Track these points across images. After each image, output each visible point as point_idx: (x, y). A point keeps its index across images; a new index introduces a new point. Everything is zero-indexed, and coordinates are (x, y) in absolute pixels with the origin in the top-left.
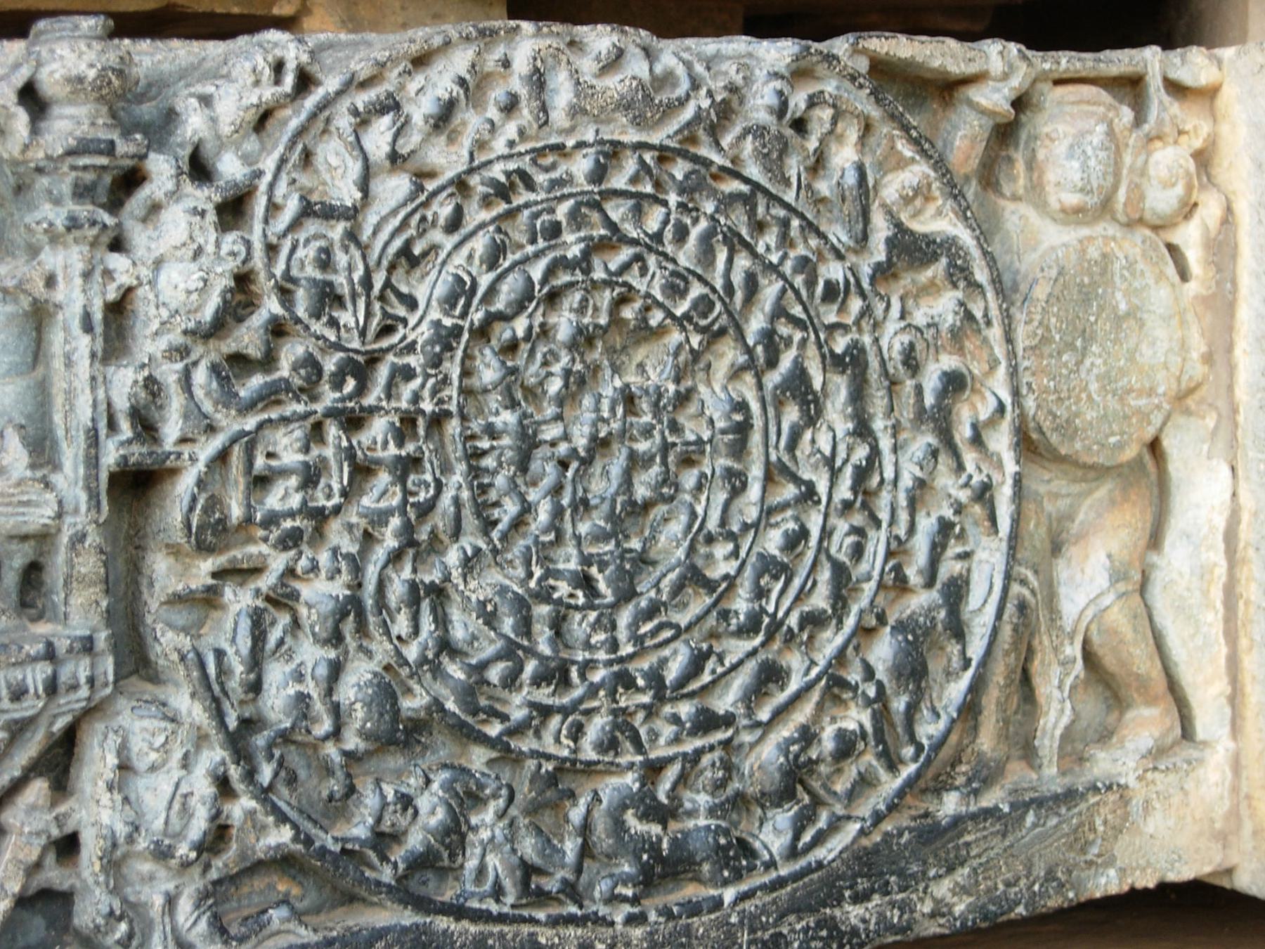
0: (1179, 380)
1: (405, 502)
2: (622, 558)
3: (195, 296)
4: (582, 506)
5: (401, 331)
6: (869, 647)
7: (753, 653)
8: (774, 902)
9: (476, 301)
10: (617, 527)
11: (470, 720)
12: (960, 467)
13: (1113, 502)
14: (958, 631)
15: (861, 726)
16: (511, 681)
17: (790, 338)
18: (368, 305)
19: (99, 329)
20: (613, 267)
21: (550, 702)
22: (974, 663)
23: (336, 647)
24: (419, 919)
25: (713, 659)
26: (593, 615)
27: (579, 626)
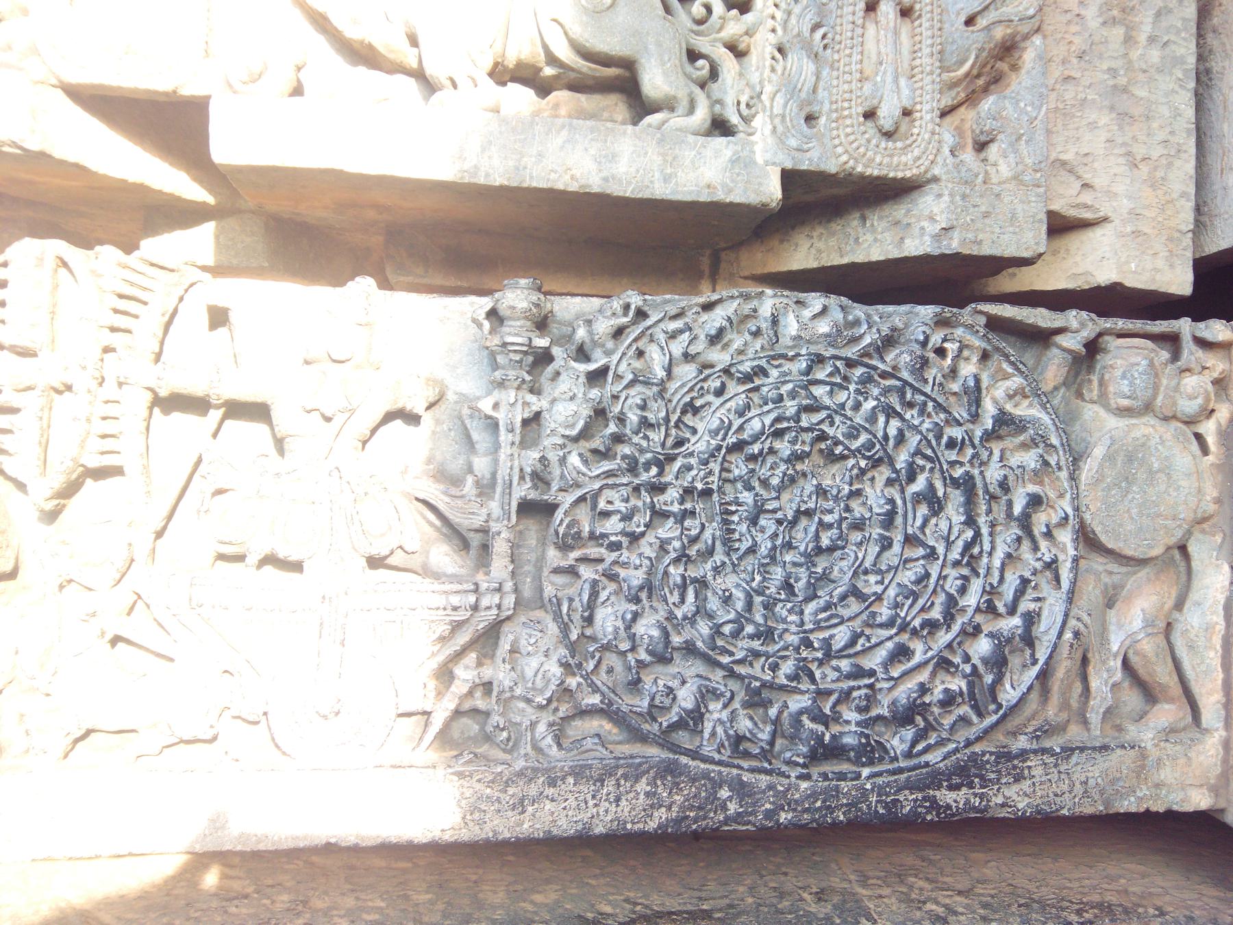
0: (1195, 512)
1: (682, 533)
2: (810, 577)
3: (570, 418)
4: (789, 546)
5: (687, 445)
7: (890, 638)
8: (895, 781)
9: (730, 433)
11: (710, 653)
12: (1036, 548)
13: (1149, 580)
14: (1029, 640)
15: (960, 688)
16: (736, 634)
19: (518, 431)
20: (814, 421)
22: (1041, 662)
23: (636, 604)
24: (671, 756)
26: (789, 605)
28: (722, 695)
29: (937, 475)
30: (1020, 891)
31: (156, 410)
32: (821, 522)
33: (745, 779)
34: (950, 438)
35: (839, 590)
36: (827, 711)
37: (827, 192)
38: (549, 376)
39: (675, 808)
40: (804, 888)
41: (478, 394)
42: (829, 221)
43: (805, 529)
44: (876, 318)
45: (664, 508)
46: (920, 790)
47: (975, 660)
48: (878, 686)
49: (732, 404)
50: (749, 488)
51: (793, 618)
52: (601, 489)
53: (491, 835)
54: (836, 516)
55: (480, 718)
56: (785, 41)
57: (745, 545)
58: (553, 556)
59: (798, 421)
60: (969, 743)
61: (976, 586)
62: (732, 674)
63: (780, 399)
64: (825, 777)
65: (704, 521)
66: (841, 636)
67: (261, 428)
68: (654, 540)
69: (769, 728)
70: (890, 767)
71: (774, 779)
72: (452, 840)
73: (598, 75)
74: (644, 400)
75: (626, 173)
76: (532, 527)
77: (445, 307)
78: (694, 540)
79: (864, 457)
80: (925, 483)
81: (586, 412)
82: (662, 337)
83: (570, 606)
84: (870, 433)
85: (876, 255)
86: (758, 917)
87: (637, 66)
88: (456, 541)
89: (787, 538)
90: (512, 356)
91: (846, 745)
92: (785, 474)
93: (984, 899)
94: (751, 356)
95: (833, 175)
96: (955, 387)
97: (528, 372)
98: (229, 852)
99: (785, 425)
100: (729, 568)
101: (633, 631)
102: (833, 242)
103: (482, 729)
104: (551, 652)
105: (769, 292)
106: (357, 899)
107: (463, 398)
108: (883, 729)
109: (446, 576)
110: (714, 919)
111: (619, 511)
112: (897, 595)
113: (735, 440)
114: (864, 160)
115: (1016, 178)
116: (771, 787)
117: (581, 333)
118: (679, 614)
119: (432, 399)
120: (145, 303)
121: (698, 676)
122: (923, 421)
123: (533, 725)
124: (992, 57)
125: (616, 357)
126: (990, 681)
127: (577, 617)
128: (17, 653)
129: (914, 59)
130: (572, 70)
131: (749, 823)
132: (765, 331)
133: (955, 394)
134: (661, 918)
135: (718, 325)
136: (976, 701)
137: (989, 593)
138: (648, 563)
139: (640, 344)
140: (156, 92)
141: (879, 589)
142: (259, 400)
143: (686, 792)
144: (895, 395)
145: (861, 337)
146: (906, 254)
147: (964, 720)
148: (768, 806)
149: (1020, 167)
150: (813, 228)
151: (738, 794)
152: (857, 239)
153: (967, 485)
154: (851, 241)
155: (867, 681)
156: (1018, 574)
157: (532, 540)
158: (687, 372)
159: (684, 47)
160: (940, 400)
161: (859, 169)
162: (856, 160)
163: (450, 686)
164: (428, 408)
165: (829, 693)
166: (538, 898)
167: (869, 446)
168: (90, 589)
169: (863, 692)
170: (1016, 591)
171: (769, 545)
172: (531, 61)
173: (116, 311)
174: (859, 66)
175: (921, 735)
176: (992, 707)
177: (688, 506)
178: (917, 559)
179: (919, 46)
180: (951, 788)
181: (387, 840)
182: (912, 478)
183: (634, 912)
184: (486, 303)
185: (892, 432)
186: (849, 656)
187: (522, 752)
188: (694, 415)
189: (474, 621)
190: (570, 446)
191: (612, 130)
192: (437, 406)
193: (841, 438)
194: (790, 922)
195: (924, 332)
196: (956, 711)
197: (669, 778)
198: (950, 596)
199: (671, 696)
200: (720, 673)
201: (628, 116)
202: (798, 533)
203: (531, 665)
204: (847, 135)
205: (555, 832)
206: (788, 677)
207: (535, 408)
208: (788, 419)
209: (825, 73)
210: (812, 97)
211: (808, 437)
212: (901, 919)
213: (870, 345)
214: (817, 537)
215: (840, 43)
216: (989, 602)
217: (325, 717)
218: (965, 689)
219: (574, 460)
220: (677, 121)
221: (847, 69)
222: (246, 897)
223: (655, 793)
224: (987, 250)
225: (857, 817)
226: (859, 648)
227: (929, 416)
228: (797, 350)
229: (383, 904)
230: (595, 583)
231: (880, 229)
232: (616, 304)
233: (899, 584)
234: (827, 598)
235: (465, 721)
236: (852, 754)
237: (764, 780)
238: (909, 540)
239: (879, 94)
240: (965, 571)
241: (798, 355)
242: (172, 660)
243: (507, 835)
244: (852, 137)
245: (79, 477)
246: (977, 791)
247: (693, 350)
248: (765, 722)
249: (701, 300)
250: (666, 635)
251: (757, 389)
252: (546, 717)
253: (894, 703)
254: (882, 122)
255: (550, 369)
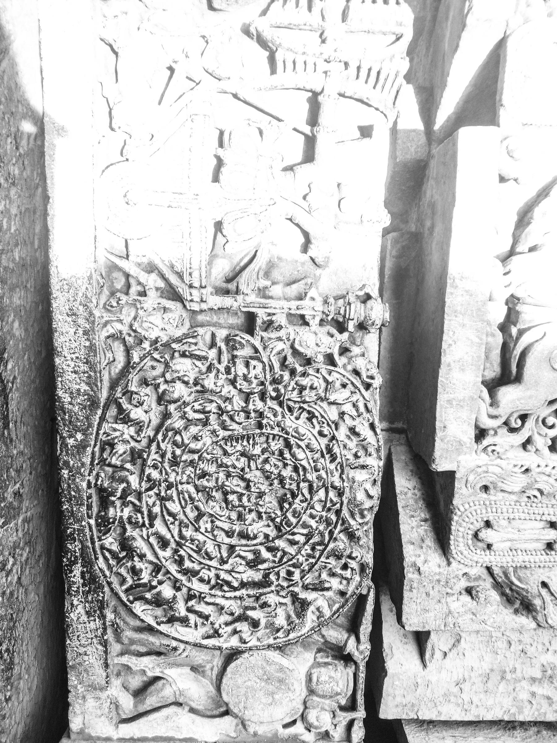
1: (236, 411)
2: (210, 488)
4: (228, 475)
6: (170, 583)
9: (296, 440)
10: (221, 488)
11: (164, 428)
12: (227, 624)
14: (171, 620)
16: (175, 443)
17: (276, 557)
18: (298, 402)
19: (299, 312)
21: (167, 458)
22: (158, 627)
24: (102, 404)
25: (173, 520)
26: (192, 476)
27: (189, 470)
28: (139, 435)
29: (271, 565)
30: (20, 615)
31: (310, 94)
32: (242, 495)
33: (88, 449)
34: (293, 573)
35: (201, 506)
36: (129, 498)
37: (441, 498)
38: (331, 331)
39: (70, 407)
40: (22, 484)
41: (320, 288)
42: (424, 500)
43: (238, 485)
44: (365, 528)
45: (251, 400)
46: (81, 555)
47: (159, 588)
48: (144, 529)
49: (314, 441)
50: (263, 451)
51: (185, 478)
52: (263, 362)
53: (54, 296)
54: (246, 504)
55: (125, 289)
56: (532, 473)
57: (229, 449)
58: (222, 334)
59: (304, 481)
60: (109, 584)
61: (204, 588)
62: (151, 441)
63: (317, 470)
64: (90, 497)
65: (244, 424)
66: (175, 507)
67: (299, 156)
68: (232, 394)
69: (119, 463)
70: (95, 537)
71: (88, 466)
72: (51, 273)
73: (512, 360)
74: (316, 388)
75: (453, 378)
76: (239, 321)
77: (372, 268)
78: (232, 418)
79: (282, 521)
80: (266, 557)
81: (309, 353)
82: (354, 398)
83: (193, 343)
84: (297, 525)
85: (404, 528)
86: (5, 457)
87: (517, 384)
88: (231, 275)
89: (233, 474)
90: (343, 308)
91: (108, 510)
92: (271, 473)
93: (16, 593)
94: (343, 453)
95: (451, 502)
96: (324, 576)
97: (333, 318)
98: (44, 137)
99: (301, 473)
100: (215, 439)
101: (177, 381)
102: (411, 502)
103: (118, 291)
104: (164, 332)
105: (381, 463)
106: (16, 215)
107: (317, 279)
108: (118, 532)
109: (211, 268)
110: (4, 431)
111: (249, 373)
112: (198, 541)
113: (292, 443)
114: (461, 521)
115: (450, 612)
116: (83, 465)
117: (356, 350)
118: (188, 409)
119: (316, 260)
120: (374, 88)
121: (150, 420)
122: (303, 556)
123: (121, 321)
124: (522, 598)
125: (342, 371)
126: (146, 596)
127: (185, 347)
128: (164, 10)
129: (521, 551)
130: (515, 345)
131: (62, 451)
132: (357, 461)
133: (320, 575)
134: (4, 398)
135: (361, 433)
136: (135, 588)
137: (200, 596)
138: (218, 390)
139: (350, 386)
140: (501, 94)
141: (203, 530)
142: (316, 156)
143: (80, 413)
144: (319, 540)
145: (354, 519)
146: (404, 546)
147: (123, 581)
148: (72, 463)
149: (456, 615)
150: (419, 490)
151: (78, 445)
152: (413, 516)
153: (265, 583)
154: (412, 513)
155: (147, 522)
156: (212, 613)
157: (233, 321)
158: (333, 414)
159: (529, 412)
160: (316, 567)
161: (455, 518)
162: (461, 516)
163: (142, 270)
164: (311, 258)
165: (140, 499)
166: (16, 324)
167: (289, 524)
168: (202, 54)
169: (140, 520)
170: (201, 612)
171: (229, 464)
172: (520, 320)
173: (370, 70)
174: (517, 517)
175: (114, 555)
176: (131, 598)
177: (253, 415)
178: (220, 553)
179: (529, 553)
180: (83, 573)
181: (51, 233)
182: (269, 549)
183: (8, 382)
184: (375, 293)
185: (297, 538)
186: (162, 512)
187: (104, 315)
188: (307, 418)
189: (183, 285)
190: (288, 344)
191: (479, 369)
192: (312, 263)
193: (293, 507)
194: (2, 476)
195: (357, 557)
196: (128, 576)
197: (88, 403)
198: (197, 573)
199: (138, 404)
200: (151, 434)
201: (487, 378)
202: (236, 481)
203: (157, 319)
204: (476, 511)
205: (56, 334)
206: (149, 475)
207: (311, 323)
208: (305, 475)
209: (514, 497)
210: (498, 489)
211: (294, 487)
212: (4, 543)
213: (350, 524)
214: (234, 492)
215: (531, 506)
216: (194, 596)
217: (125, 196)
218: (142, 581)
219: (280, 346)
220: (484, 407)
221: (516, 510)
222: (17, 148)
223: (79, 395)
224: (406, 594)
225: (65, 516)
226: (167, 517)
227: (307, 560)
228: (346, 480)
229: (12, 231)
230: (206, 358)
231: (419, 530)
232: (374, 371)
233: (205, 542)
234: (197, 499)
235: (123, 280)
236: (103, 514)
237: (87, 460)
238: (232, 548)
239: (500, 530)
240: (213, 582)
241: (343, 481)
242: (160, 103)
243: (54, 306)
244: (474, 513)
245: (269, 47)
246: (81, 588)
247: (346, 417)
248: (122, 461)
249: (377, 422)
250: (175, 402)
251: (323, 456)
252: (125, 329)
253: (134, 539)
254: (484, 531)
255: (334, 331)
